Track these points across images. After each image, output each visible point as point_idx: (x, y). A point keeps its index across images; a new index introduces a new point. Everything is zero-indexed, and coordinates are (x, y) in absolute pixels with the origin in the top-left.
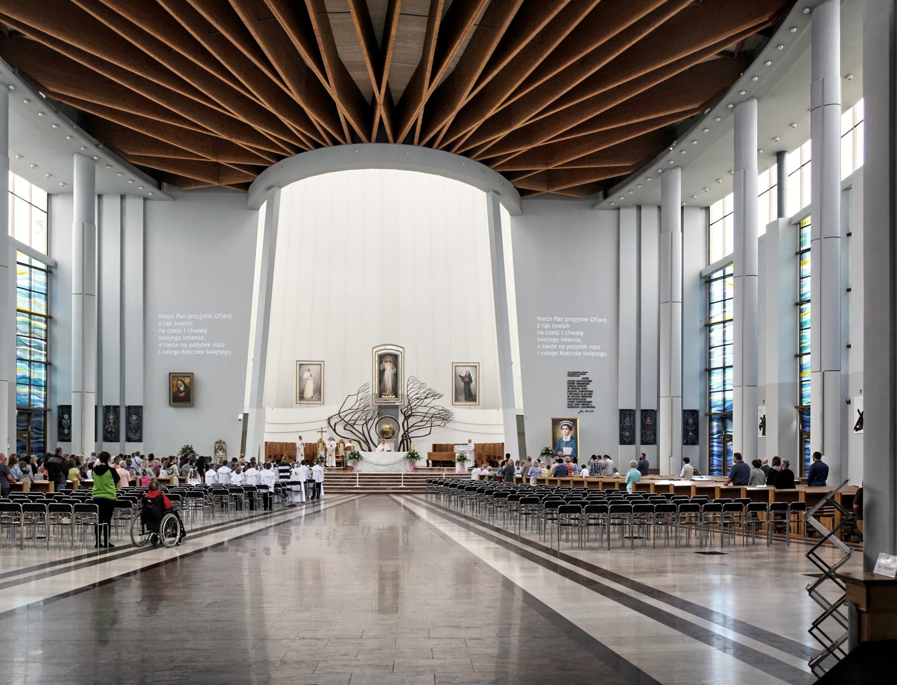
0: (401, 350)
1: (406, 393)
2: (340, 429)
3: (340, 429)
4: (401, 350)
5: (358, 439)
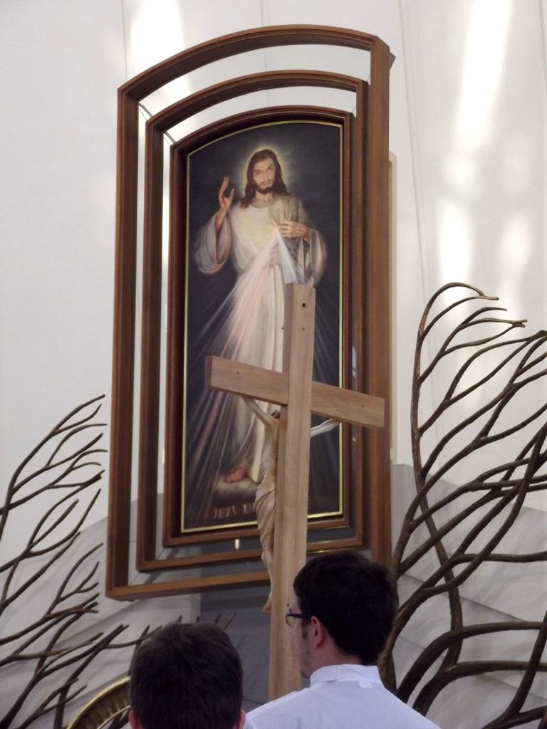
0: (356, 64)
4: (356, 64)
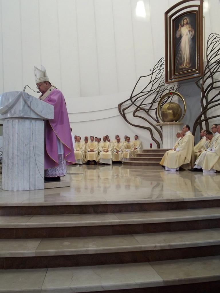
2: (129, 116)
5: (147, 125)
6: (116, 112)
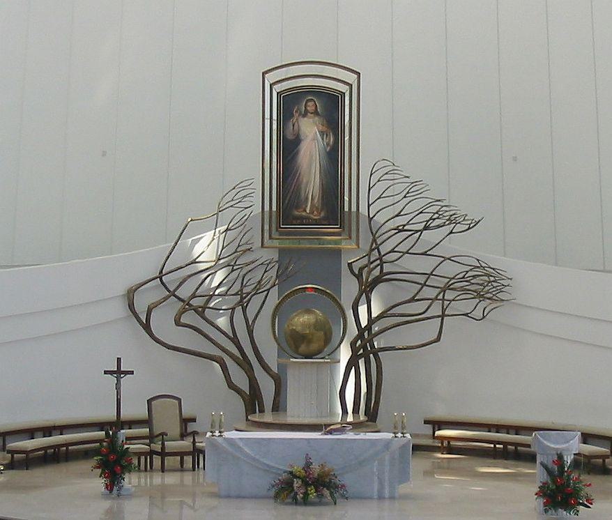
0: (351, 78)
1: (363, 209)
2: (163, 322)
3: (163, 322)
4: (351, 78)
5: (217, 352)
6: (120, 309)
